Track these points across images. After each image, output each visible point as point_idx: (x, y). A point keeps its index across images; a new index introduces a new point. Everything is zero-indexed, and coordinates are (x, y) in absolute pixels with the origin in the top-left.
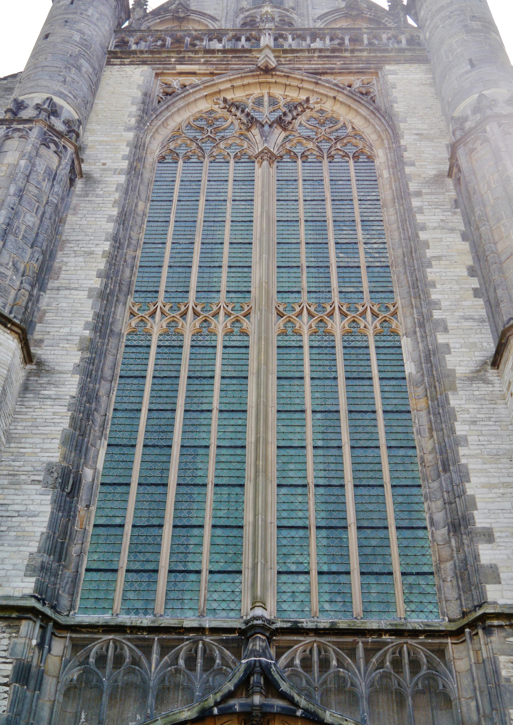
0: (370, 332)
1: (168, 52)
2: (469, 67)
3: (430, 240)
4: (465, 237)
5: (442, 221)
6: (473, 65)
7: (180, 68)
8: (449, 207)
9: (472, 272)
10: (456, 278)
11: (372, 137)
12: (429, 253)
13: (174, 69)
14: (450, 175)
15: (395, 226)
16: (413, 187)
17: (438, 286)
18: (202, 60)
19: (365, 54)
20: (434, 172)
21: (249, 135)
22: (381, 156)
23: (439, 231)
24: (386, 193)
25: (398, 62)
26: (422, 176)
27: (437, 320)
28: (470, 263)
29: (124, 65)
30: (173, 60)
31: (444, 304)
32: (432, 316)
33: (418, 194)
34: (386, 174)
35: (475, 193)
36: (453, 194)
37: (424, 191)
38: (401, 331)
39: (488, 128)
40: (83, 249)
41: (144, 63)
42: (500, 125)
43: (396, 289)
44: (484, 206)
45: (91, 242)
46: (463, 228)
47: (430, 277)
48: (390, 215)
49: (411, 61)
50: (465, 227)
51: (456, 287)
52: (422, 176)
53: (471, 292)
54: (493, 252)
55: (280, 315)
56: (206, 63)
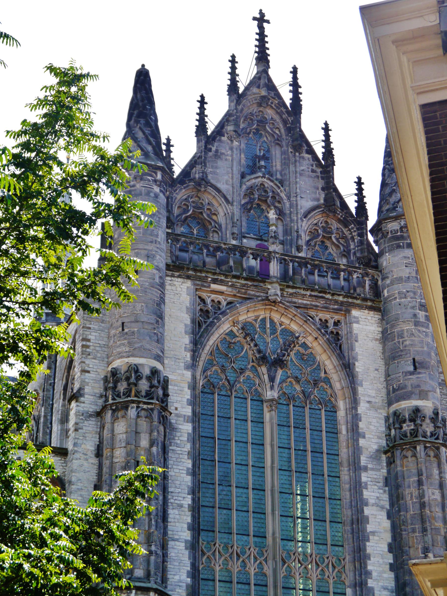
0: (331, 581)
1: (207, 272)
2: (411, 368)
3: (370, 516)
4: (389, 517)
5: (378, 497)
6: (415, 368)
7: (214, 286)
8: (381, 484)
9: (391, 549)
10: (381, 553)
11: (337, 386)
12: (370, 528)
13: (209, 287)
14: (385, 452)
15: (347, 486)
16: (364, 460)
17: (372, 559)
18: (230, 283)
19: (341, 298)
20: (375, 447)
21: (259, 369)
22: (341, 405)
23: (375, 508)
24: (344, 453)
25: (360, 307)
26: (369, 450)
27: (370, 587)
28: (390, 540)
29: (174, 277)
30: (210, 279)
31: (374, 574)
32: (367, 584)
33: (366, 469)
34: (344, 432)
35: (402, 498)
36: (385, 471)
37: (370, 466)
38: (347, 584)
39: (418, 448)
40: (176, 502)
41: (188, 277)
42: (426, 447)
43: (346, 546)
44: (407, 512)
45: (180, 495)
46: (388, 507)
47: (369, 550)
48: (345, 475)
49: (371, 308)
50: (390, 507)
51: (381, 561)
52: (369, 450)
53: (388, 566)
54: (407, 555)
55: (284, 562)
56: (232, 286)
